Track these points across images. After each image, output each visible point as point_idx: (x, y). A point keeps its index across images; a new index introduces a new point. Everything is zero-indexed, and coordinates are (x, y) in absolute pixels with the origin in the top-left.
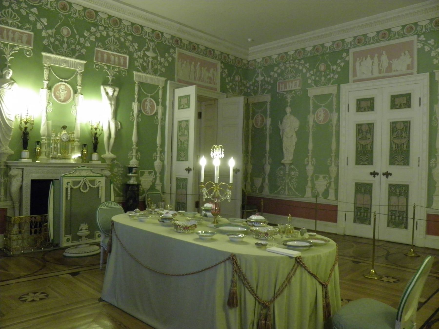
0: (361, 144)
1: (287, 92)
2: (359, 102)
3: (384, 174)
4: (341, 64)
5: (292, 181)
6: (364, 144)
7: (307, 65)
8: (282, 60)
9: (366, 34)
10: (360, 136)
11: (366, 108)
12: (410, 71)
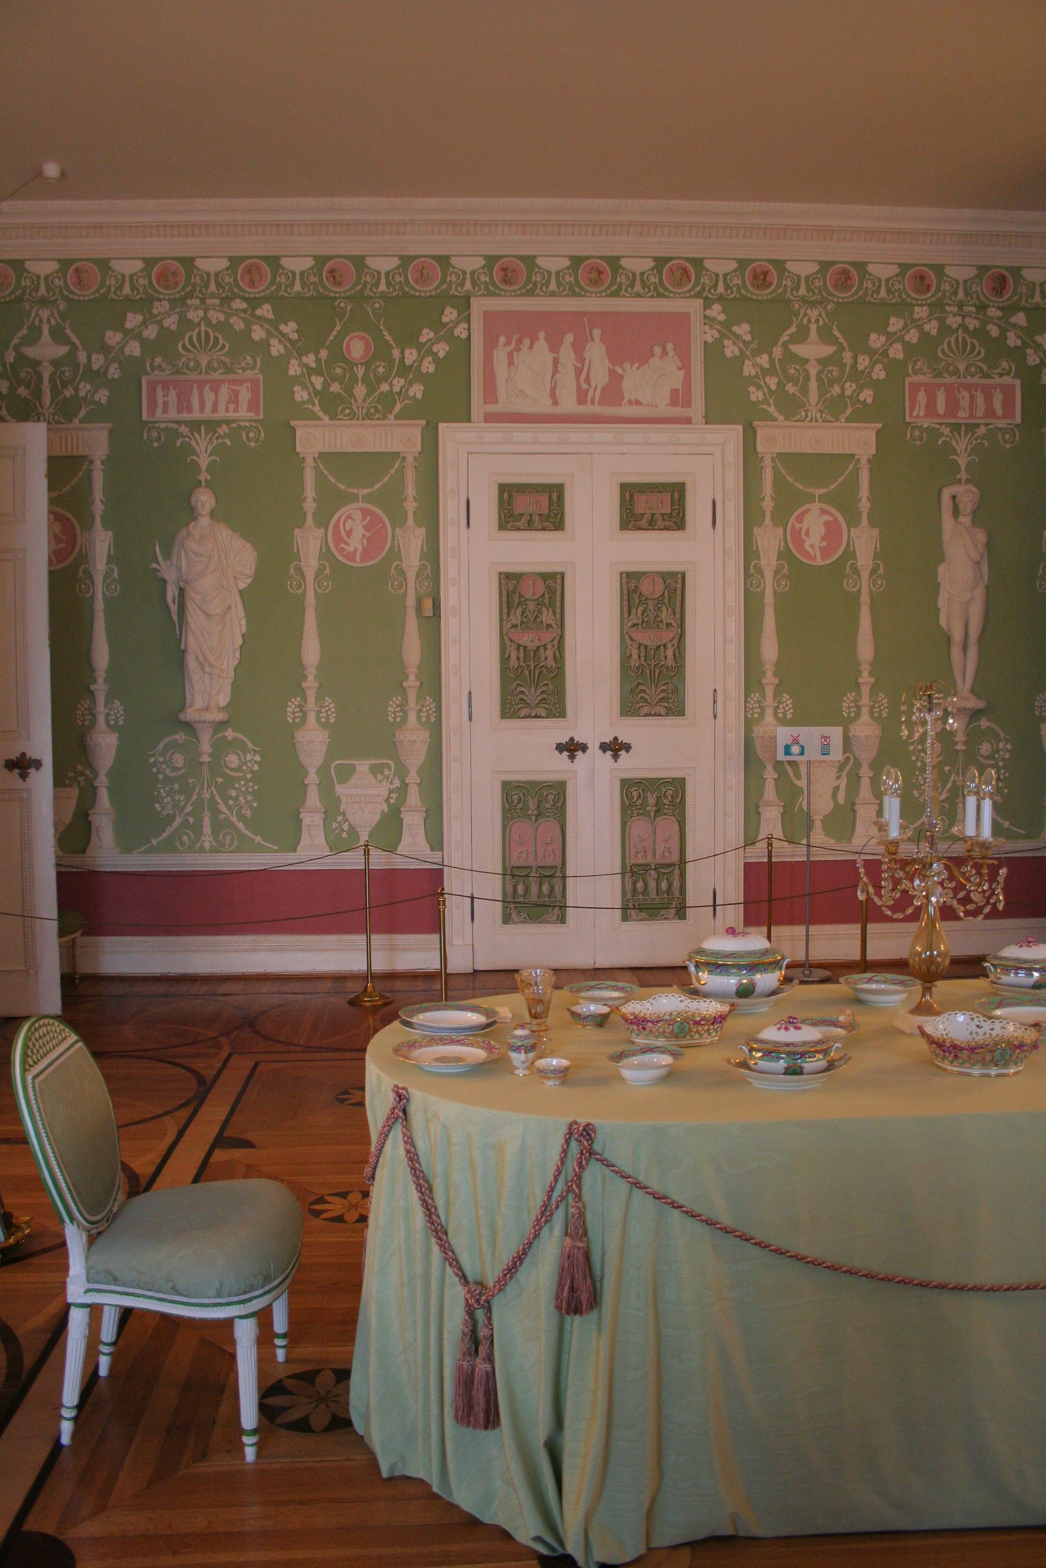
0: (519, 646)
1: (195, 426)
2: (508, 493)
3: (604, 747)
4: (435, 349)
5: (234, 793)
6: (532, 646)
7: (290, 328)
8: (168, 287)
9: (535, 257)
10: (516, 617)
11: (537, 518)
12: (677, 411)
